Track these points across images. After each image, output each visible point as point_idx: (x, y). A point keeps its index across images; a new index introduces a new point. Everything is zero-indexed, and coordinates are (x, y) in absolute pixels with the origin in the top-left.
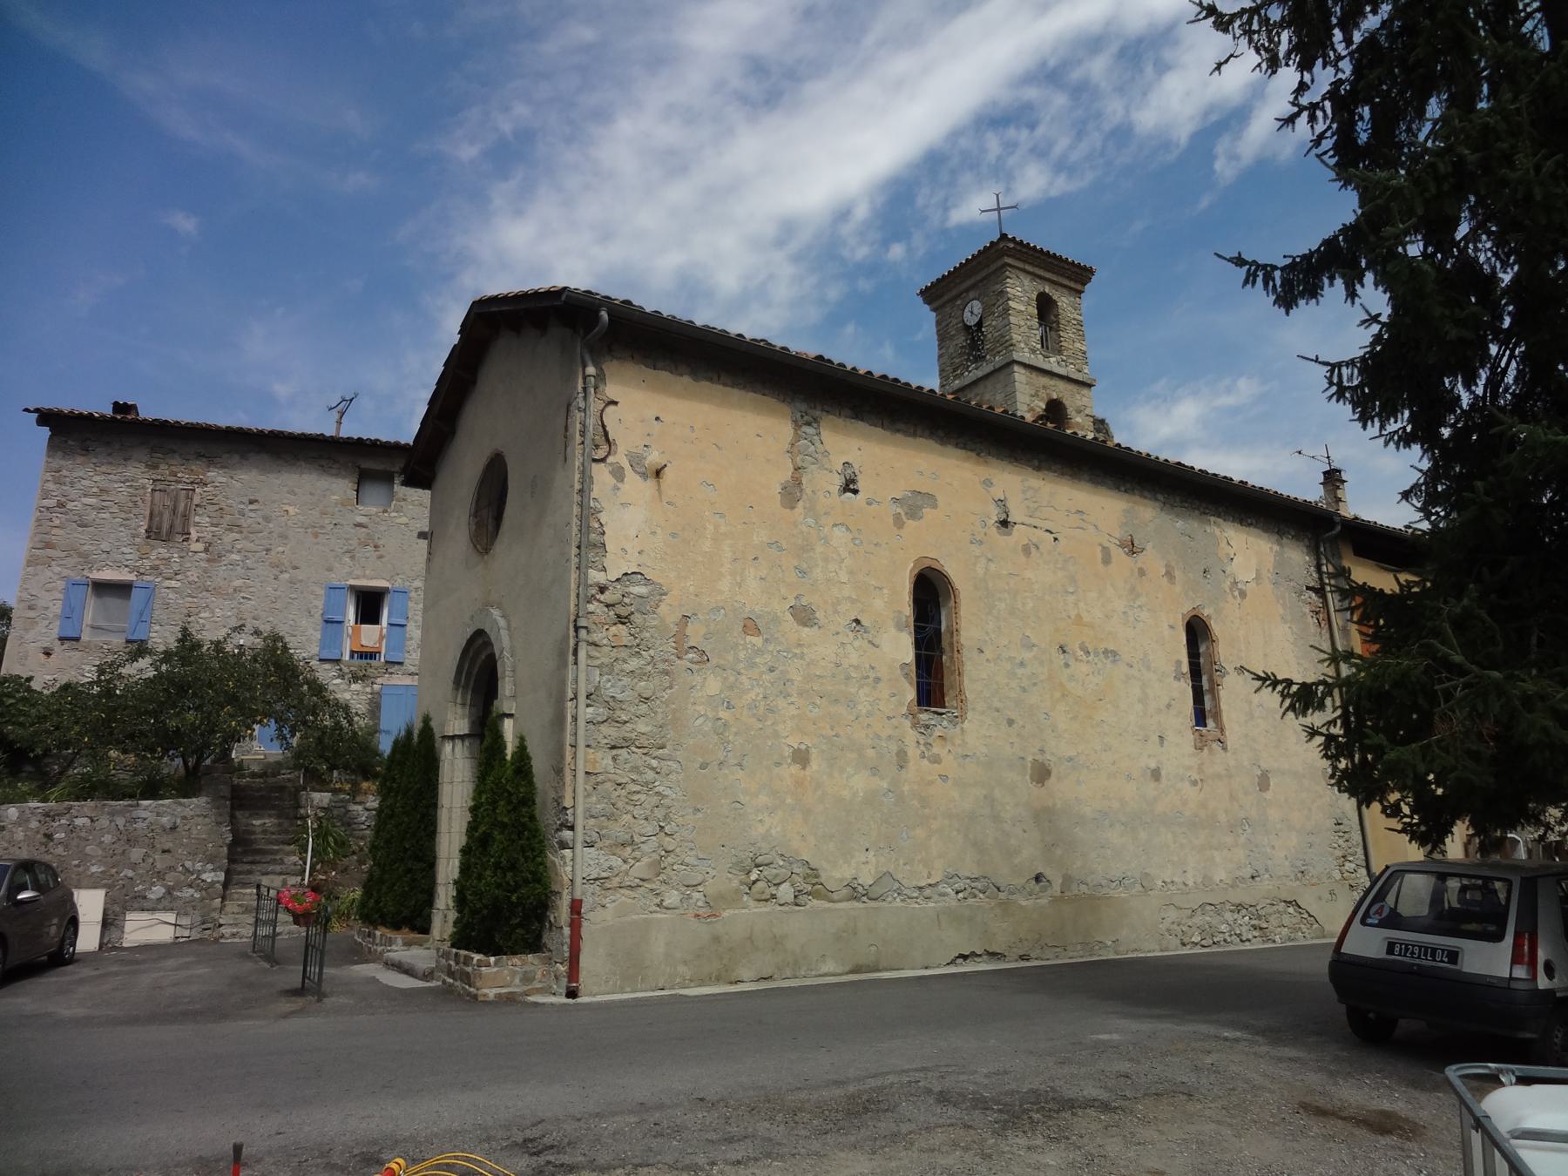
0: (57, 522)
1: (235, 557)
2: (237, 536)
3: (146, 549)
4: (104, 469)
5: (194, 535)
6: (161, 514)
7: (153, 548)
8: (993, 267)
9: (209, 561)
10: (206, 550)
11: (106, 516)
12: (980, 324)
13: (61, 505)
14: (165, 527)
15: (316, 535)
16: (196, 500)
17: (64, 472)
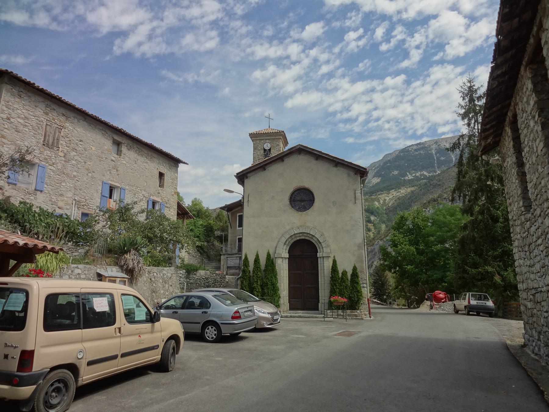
0: (6, 126)
1: (74, 162)
2: (75, 154)
3: (42, 150)
4: (27, 107)
5: (61, 149)
6: (49, 136)
7: (45, 150)
8: (277, 137)
9: (65, 161)
10: (64, 157)
11: (27, 130)
12: (270, 150)
13: (8, 119)
14: (51, 141)
15: (100, 161)
16: (62, 134)
17: (10, 103)
